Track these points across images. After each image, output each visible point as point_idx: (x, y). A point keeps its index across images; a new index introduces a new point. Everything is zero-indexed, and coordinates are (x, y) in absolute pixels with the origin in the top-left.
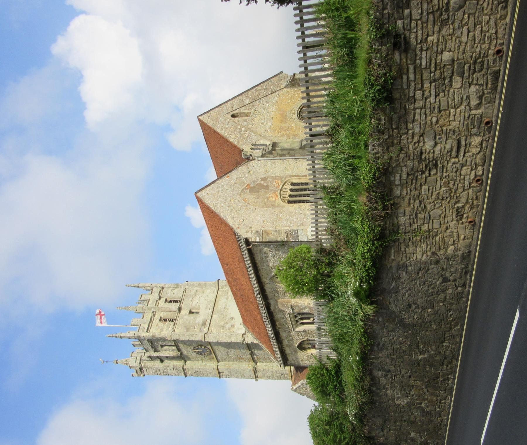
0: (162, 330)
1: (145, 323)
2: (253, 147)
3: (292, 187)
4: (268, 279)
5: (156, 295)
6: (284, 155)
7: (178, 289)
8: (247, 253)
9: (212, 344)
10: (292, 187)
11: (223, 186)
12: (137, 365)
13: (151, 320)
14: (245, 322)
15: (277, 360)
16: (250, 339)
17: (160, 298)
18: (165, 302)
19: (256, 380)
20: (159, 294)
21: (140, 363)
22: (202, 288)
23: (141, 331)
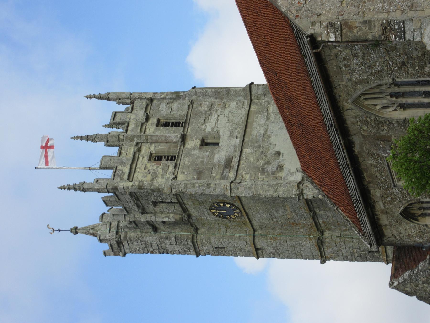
0: (155, 176)
1: (123, 164)
4: (349, 101)
5: (140, 114)
7: (179, 102)
8: (313, 60)
9: (243, 200)
12: (112, 235)
13: (134, 159)
14: (305, 168)
15: (364, 235)
16: (311, 192)
17: (147, 118)
18: (157, 125)
19: (323, 262)
20: (145, 111)
21: (117, 233)
22: (222, 99)
23: (117, 180)
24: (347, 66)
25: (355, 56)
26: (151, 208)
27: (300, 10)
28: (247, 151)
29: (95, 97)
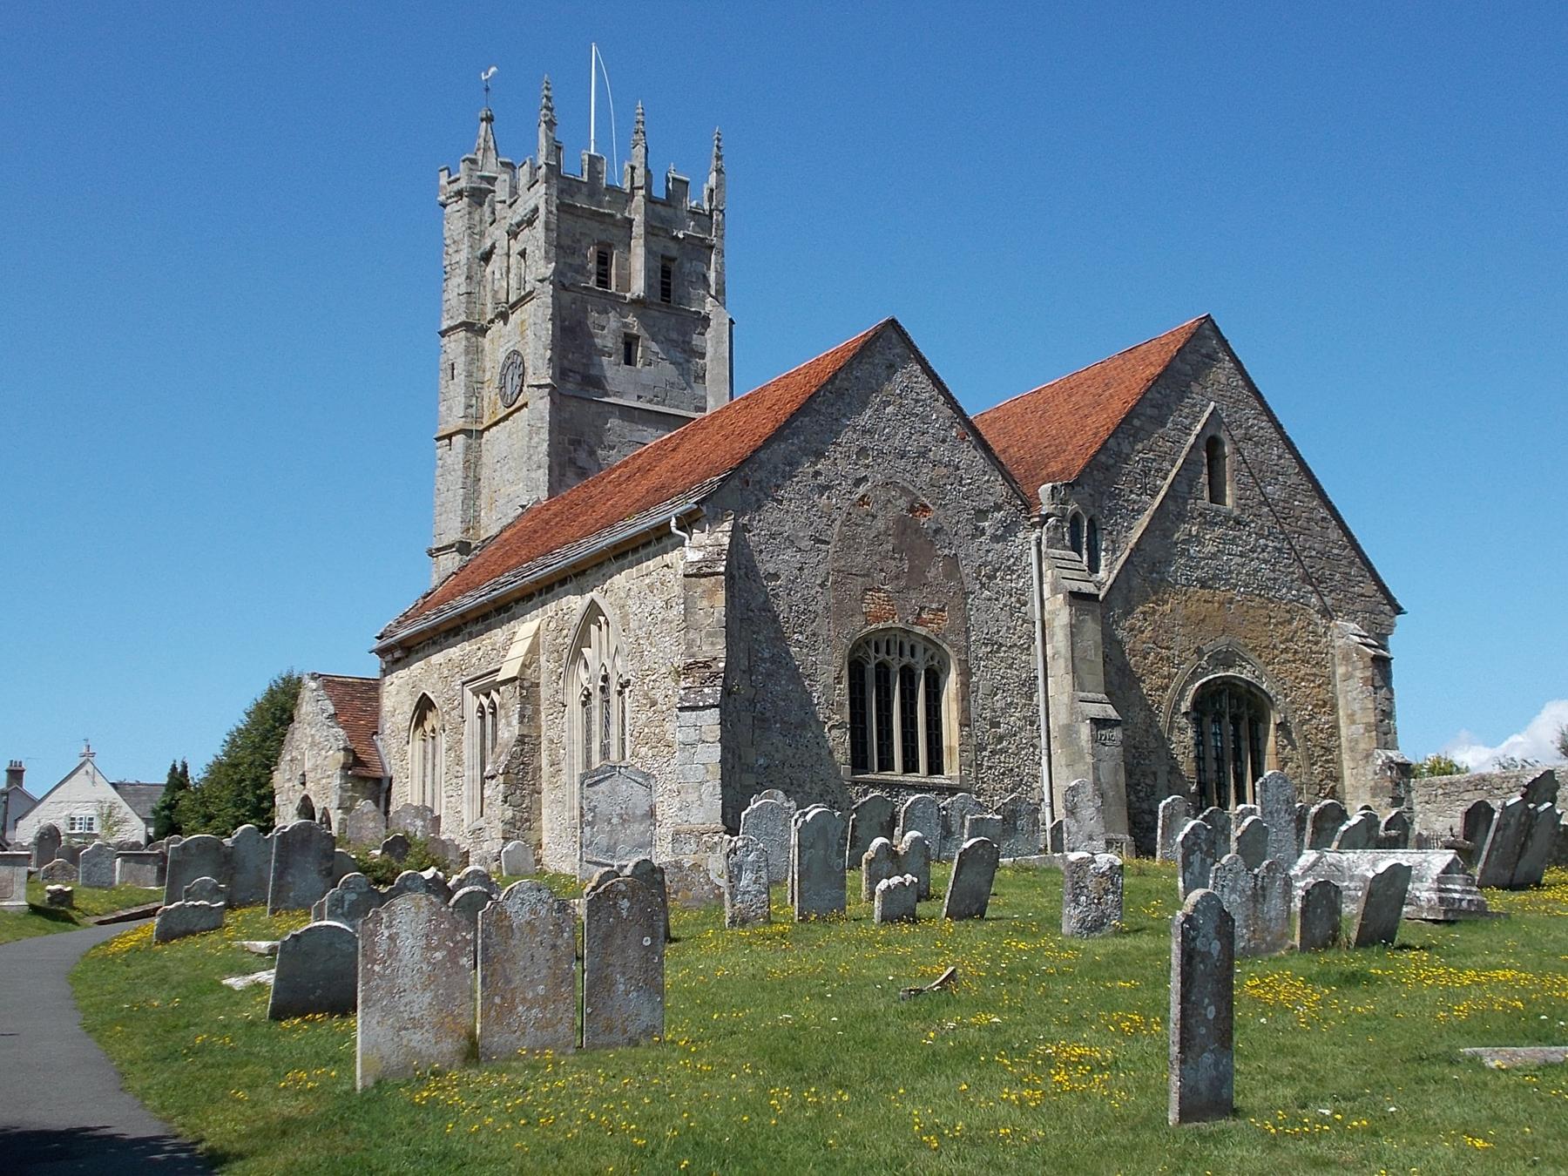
24: (651, 587)
25: (668, 605)
26: (516, 247)
27: (761, 489)
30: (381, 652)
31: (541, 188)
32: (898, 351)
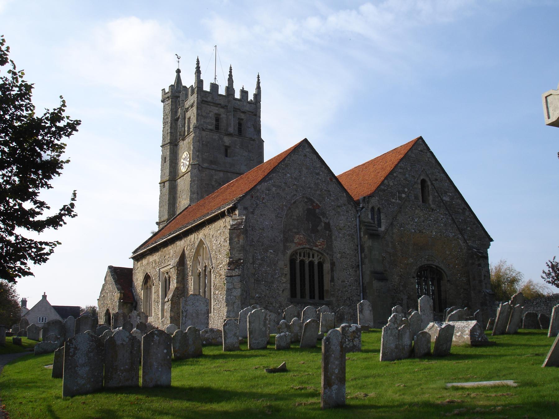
1: (213, 98)
2: (376, 209)
3: (316, 263)
5: (247, 108)
6: (362, 250)
10: (316, 263)
11: (318, 174)
17: (244, 112)
28: (221, 174)
29: (259, 80)
30: (133, 258)
31: (195, 95)
32: (308, 150)
